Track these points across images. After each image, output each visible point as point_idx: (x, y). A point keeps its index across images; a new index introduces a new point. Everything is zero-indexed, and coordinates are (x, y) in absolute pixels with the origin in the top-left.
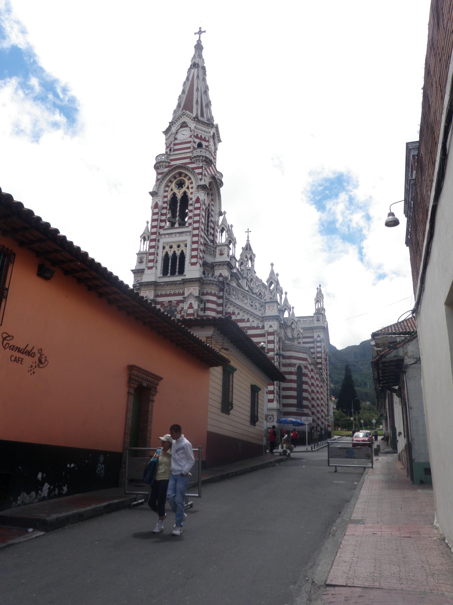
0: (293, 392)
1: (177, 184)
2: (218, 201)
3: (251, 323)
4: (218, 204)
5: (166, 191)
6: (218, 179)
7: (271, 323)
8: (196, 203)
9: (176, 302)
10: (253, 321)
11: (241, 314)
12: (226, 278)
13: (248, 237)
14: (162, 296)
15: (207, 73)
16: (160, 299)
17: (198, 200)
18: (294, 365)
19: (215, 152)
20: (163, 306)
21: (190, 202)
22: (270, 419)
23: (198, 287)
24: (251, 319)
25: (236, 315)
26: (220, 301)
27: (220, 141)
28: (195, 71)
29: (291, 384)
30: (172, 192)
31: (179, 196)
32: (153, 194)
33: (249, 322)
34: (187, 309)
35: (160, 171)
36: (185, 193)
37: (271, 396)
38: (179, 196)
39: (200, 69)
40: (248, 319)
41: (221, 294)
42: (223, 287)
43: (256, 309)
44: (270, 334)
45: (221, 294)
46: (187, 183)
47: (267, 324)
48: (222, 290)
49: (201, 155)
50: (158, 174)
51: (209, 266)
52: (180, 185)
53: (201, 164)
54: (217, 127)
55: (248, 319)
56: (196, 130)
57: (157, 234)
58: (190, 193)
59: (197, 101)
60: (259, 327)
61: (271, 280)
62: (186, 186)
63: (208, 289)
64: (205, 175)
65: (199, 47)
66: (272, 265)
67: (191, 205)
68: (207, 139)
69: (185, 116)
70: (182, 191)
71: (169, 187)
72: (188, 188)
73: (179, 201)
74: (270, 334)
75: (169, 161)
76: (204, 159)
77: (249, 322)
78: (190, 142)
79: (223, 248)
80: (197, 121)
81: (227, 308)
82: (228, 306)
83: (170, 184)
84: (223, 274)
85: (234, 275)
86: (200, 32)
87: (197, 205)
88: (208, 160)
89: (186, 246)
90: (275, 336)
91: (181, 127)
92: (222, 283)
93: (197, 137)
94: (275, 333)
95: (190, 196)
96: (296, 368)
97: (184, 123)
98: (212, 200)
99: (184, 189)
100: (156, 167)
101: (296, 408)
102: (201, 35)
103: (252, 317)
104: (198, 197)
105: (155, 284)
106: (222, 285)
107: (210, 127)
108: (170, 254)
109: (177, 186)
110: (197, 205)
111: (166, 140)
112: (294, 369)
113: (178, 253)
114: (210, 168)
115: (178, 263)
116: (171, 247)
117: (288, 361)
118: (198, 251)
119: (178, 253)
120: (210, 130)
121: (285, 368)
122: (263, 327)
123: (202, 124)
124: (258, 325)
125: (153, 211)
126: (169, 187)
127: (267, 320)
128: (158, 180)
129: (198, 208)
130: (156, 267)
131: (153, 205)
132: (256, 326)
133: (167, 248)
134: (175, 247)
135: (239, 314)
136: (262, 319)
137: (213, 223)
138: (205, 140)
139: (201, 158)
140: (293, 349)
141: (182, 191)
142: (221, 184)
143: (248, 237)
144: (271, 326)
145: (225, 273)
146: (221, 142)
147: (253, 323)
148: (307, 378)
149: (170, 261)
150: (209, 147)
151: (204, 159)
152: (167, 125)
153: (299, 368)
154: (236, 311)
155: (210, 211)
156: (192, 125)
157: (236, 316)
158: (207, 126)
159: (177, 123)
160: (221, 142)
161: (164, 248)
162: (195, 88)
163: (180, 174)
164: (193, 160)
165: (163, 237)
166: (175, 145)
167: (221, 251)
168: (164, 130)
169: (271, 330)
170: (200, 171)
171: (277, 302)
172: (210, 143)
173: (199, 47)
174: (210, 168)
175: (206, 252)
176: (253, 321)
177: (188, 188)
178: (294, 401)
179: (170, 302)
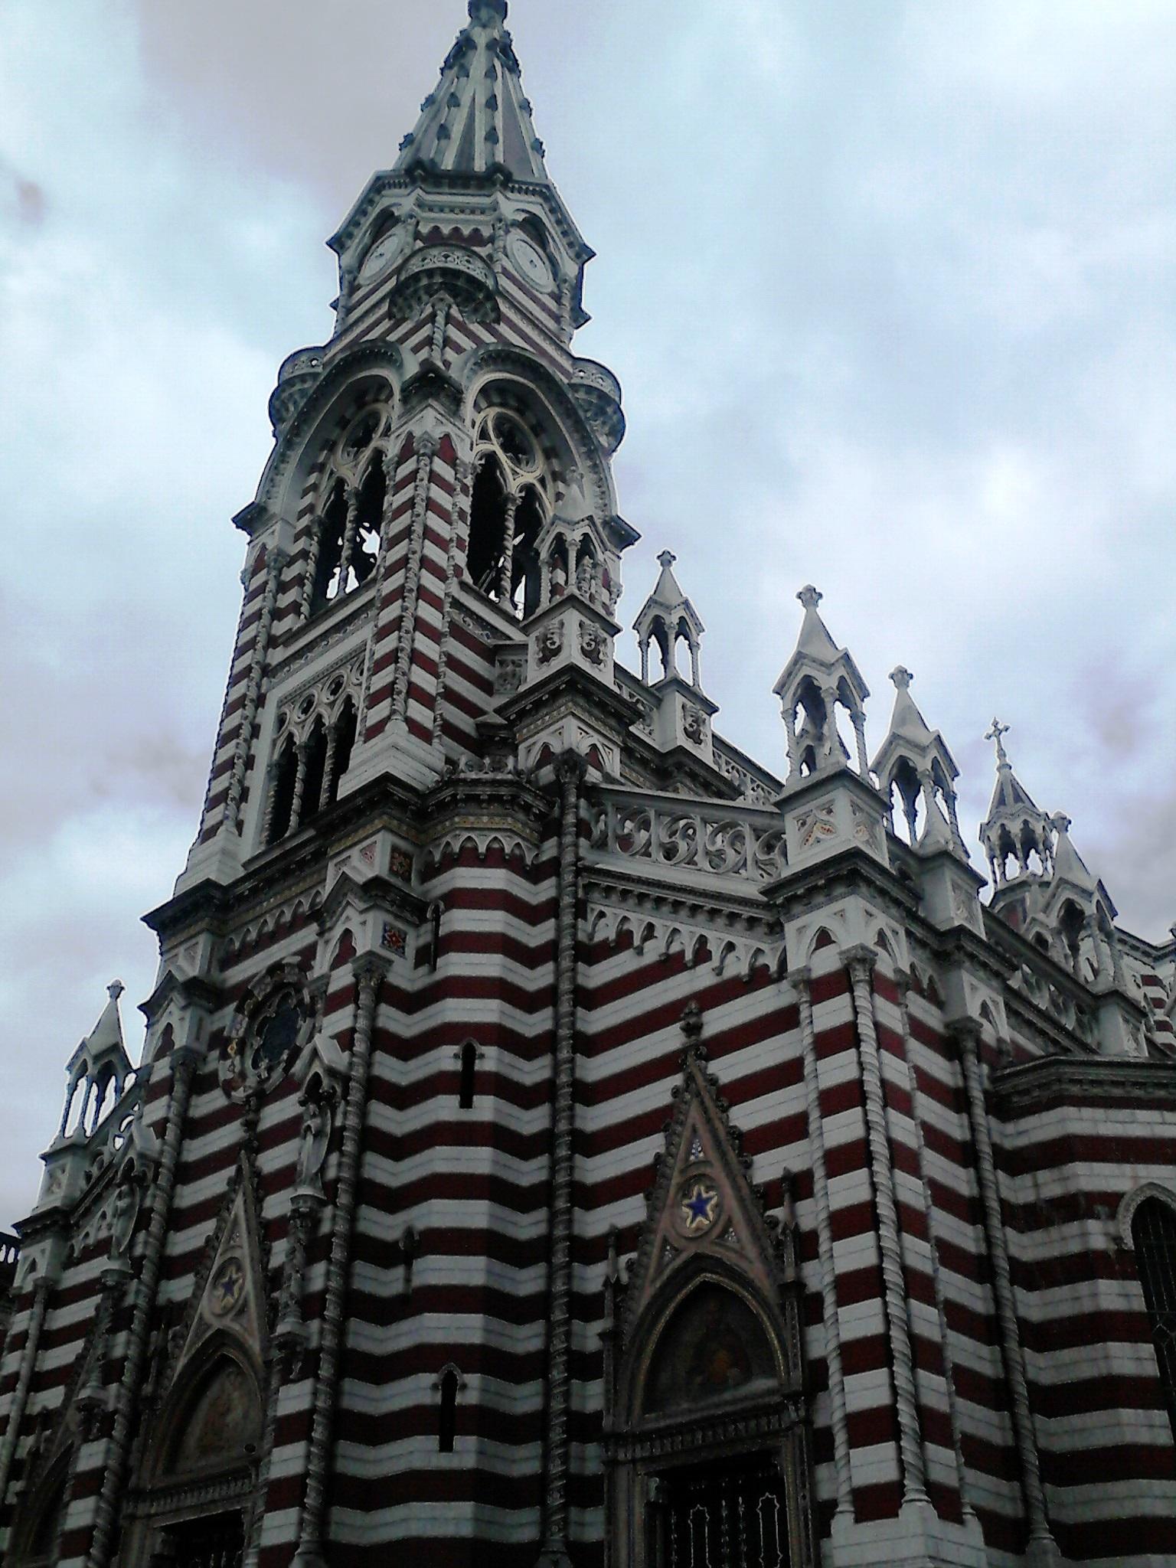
3: (715, 962)
7: (820, 917)
9: (298, 958)
10: (730, 947)
11: (663, 924)
14: (249, 950)
16: (237, 974)
20: (249, 1005)
25: (637, 942)
26: (542, 892)
34: (325, 969)
37: (873, 1464)
40: (702, 940)
41: (549, 849)
44: (822, 989)
45: (549, 849)
48: (549, 827)
60: (767, 967)
61: (806, 671)
64: (447, 341)
66: (810, 597)
68: (486, 232)
70: (367, 453)
71: (321, 468)
74: (822, 989)
81: (591, 917)
84: (557, 748)
85: (679, 766)
88: (460, 283)
90: (862, 991)
92: (556, 790)
94: (860, 974)
96: (1125, 1228)
98: (556, 476)
99: (376, 442)
103: (721, 921)
104: (410, 435)
106: (555, 801)
117: (1050, 1184)
119: (330, 718)
124: (761, 961)
125: (246, 590)
126: (321, 468)
127: (797, 909)
130: (239, 825)
131: (252, 562)
133: (294, 715)
135: (650, 931)
136: (766, 916)
139: (424, 282)
140: (1075, 1090)
141: (367, 453)
144: (824, 938)
145: (572, 732)
147: (731, 957)
157: (640, 951)
161: (281, 721)
165: (281, 675)
169: (826, 963)
171: (844, 775)
174: (503, 328)
176: (730, 947)
179: (276, 968)
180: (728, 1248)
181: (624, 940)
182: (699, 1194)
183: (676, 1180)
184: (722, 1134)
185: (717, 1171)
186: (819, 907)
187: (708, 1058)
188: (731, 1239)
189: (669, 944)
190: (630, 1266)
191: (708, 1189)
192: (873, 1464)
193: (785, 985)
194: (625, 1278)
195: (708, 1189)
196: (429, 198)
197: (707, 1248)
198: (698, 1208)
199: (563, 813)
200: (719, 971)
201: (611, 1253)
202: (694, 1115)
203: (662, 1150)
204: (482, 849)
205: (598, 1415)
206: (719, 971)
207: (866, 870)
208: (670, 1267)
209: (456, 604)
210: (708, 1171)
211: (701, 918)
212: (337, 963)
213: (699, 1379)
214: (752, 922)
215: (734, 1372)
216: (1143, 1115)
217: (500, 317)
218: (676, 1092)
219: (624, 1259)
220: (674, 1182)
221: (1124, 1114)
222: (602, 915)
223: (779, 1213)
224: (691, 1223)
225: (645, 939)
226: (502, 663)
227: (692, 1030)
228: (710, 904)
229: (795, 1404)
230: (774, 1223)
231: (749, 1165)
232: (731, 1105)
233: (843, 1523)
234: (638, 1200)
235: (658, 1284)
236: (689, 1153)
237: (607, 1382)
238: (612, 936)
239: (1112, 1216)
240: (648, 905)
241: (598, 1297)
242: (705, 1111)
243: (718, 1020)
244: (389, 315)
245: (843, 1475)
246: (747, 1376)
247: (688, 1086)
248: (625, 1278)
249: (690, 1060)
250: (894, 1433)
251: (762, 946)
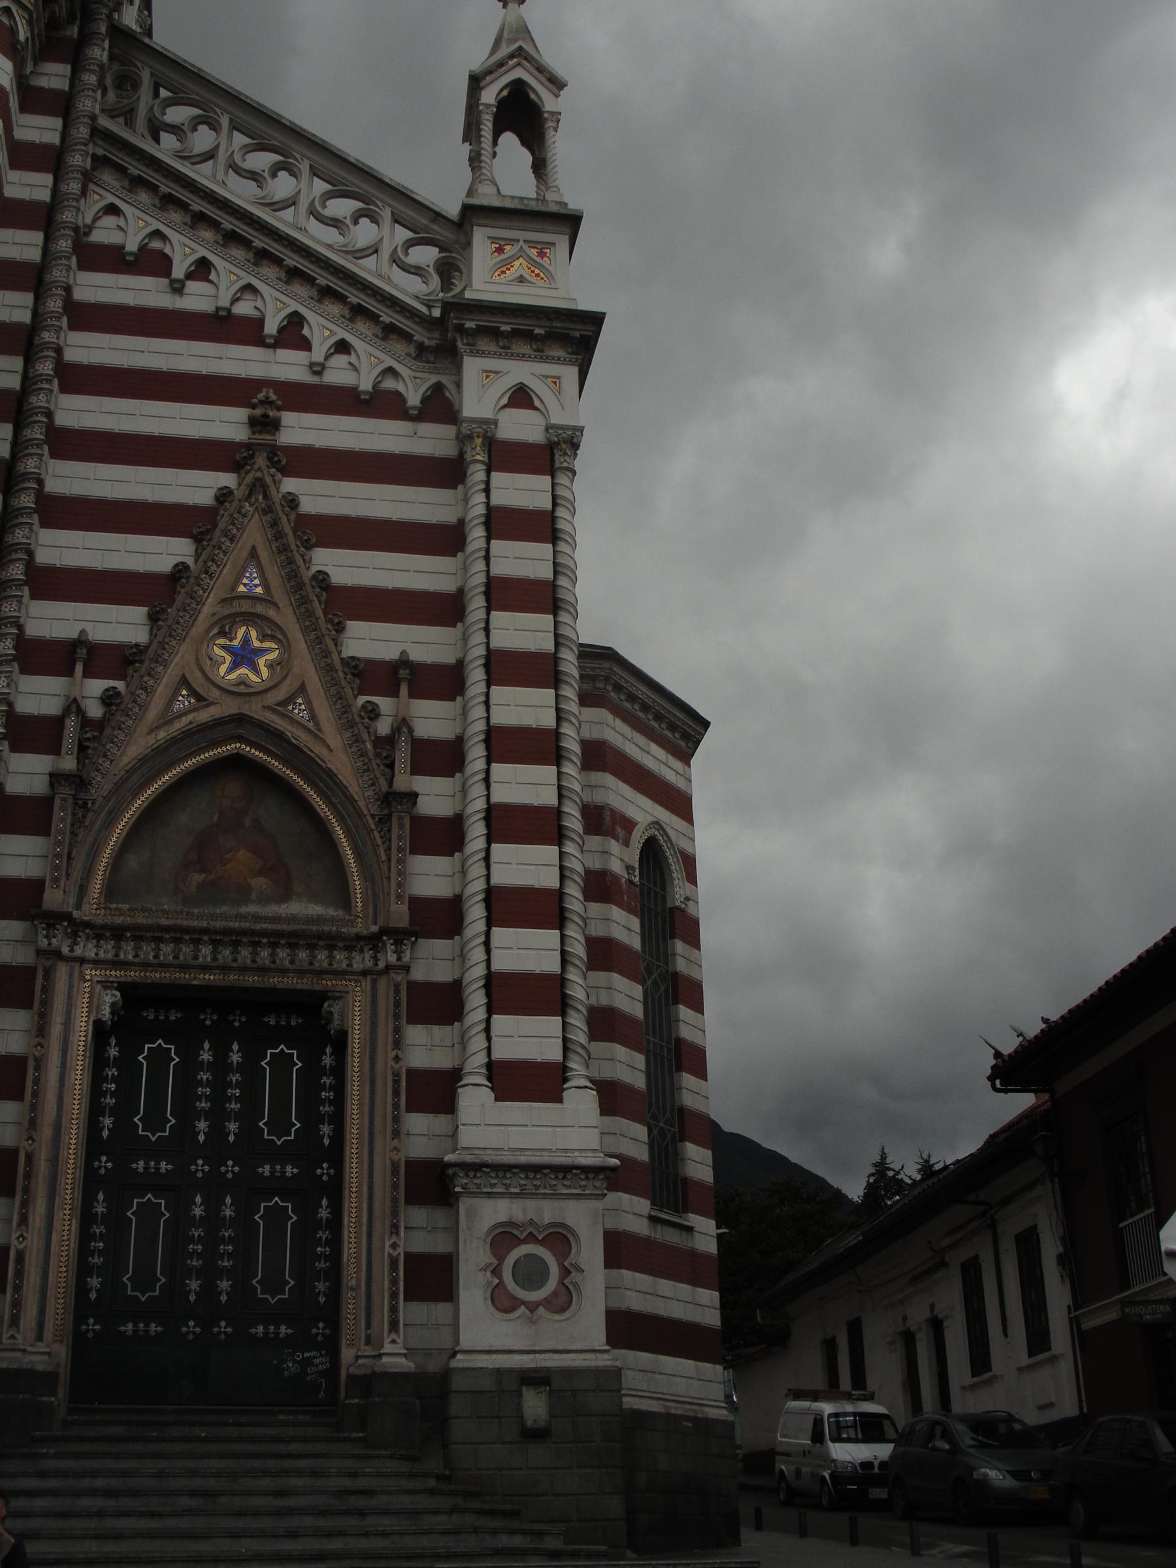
22: (531, 1274)
24: (322, 328)
25: (178, 272)
37: (529, 1037)
40: (295, 321)
55: (295, 321)
60: (398, 398)
101: (643, 1205)
122: (439, 407)
124: (389, 384)
127: (484, 344)
135: (202, 269)
136: (420, 335)
144: (521, 397)
147: (340, 360)
157: (177, 288)
169: (519, 427)
176: (342, 347)
180: (293, 721)
181: (151, 262)
182: (246, 641)
183: (210, 608)
184: (307, 575)
185: (288, 619)
186: (522, 357)
187: (287, 472)
188: (300, 711)
189: (235, 300)
190: (109, 699)
191: (263, 637)
192: (529, 1037)
194: (95, 710)
195: (263, 637)
197: (254, 710)
198: (244, 656)
200: (317, 369)
201: (79, 668)
202: (254, 534)
203: (190, 561)
205: (36, 887)
206: (317, 369)
208: (185, 720)
210: (271, 613)
213: (198, 878)
214: (390, 331)
215: (259, 883)
218: (224, 496)
219: (97, 686)
220: (206, 610)
221: (642, 740)
222: (112, 210)
223: (385, 704)
224: (225, 672)
225: (190, 276)
227: (264, 424)
229: (398, 943)
230: (373, 713)
231: (340, 628)
232: (321, 544)
233: (475, 1099)
234: (142, 611)
235: (162, 734)
236: (237, 581)
237: (59, 843)
238: (132, 246)
241: (57, 723)
242: (279, 536)
243: (301, 429)
245: (478, 1042)
246: (286, 896)
247: (250, 495)
248: (95, 710)
249: (261, 461)
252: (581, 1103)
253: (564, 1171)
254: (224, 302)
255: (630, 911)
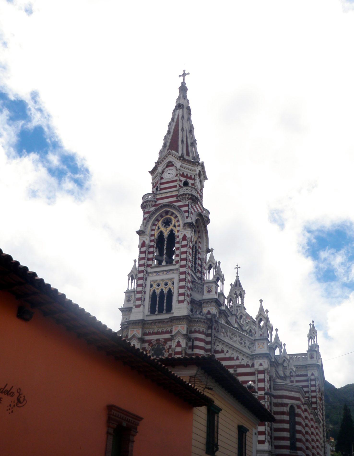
0: (285, 433)
1: (164, 223)
2: (205, 238)
3: (240, 361)
4: (205, 241)
5: (153, 230)
6: (205, 216)
7: (261, 361)
8: (183, 240)
9: (164, 340)
12: (214, 316)
13: (237, 273)
14: (149, 334)
15: (191, 113)
16: (148, 338)
17: (184, 238)
18: (286, 405)
19: (201, 190)
20: (151, 345)
21: (177, 240)
23: (185, 325)
24: (240, 357)
25: (225, 352)
26: (209, 339)
27: (206, 178)
28: (180, 112)
29: (283, 424)
30: (159, 230)
31: (166, 234)
32: (140, 233)
33: (238, 359)
34: (174, 347)
35: (147, 210)
36: (172, 231)
37: (262, 438)
38: (166, 234)
39: (185, 109)
40: (238, 357)
41: (209, 331)
42: (211, 325)
43: (245, 346)
44: (260, 372)
45: (209, 331)
46: (174, 221)
47: (257, 363)
48: (210, 328)
49: (187, 193)
50: (145, 213)
51: (197, 304)
52: (167, 223)
53: (187, 202)
54: (202, 165)
55: (238, 357)
56: (182, 169)
57: (145, 273)
58: (177, 231)
59: (182, 141)
60: (249, 365)
62: (173, 224)
63: (196, 327)
64: (191, 212)
65: (183, 89)
66: (261, 301)
67: (178, 242)
68: (193, 177)
69: (170, 156)
70: (169, 229)
71: (156, 225)
72: (175, 226)
73: (166, 239)
74: (260, 372)
75: (155, 200)
76: (190, 196)
77: (238, 359)
78: (176, 181)
79: (211, 285)
80: (182, 160)
81: (216, 345)
82: (217, 343)
83: (156, 223)
84: (211, 312)
86: (184, 75)
87: (184, 243)
88: (194, 198)
89: (173, 284)
90: (266, 374)
91: (167, 166)
92: (211, 320)
93: (183, 175)
94: (266, 372)
95: (177, 234)
97: (170, 162)
98: (199, 237)
99: (171, 227)
100: (143, 206)
101: (289, 451)
102: (185, 77)
103: (241, 355)
104: (185, 235)
105: (142, 322)
107: (196, 165)
108: (158, 292)
109: (164, 225)
110: (184, 243)
111: (153, 179)
112: (286, 409)
113: (166, 291)
114: (197, 205)
115: (165, 301)
116: (158, 285)
117: (280, 401)
118: (185, 288)
119: (166, 291)
120: (196, 168)
121: (277, 408)
122: (253, 366)
123: (187, 163)
124: (248, 363)
125: (140, 250)
126: (156, 225)
128: (144, 219)
129: (185, 246)
130: (144, 306)
131: (141, 244)
132: (245, 364)
133: (155, 286)
134: (162, 284)
135: (227, 352)
137: (201, 261)
138: (191, 178)
139: (187, 196)
140: (285, 388)
141: (169, 229)
142: (208, 221)
143: (237, 273)
144: (261, 365)
146: (207, 179)
147: (243, 361)
148: (300, 418)
149: (158, 299)
150: (195, 185)
151: (190, 196)
152: (153, 165)
153: (292, 407)
154: (225, 349)
155: (198, 248)
156: (178, 164)
157: (225, 355)
158: (193, 164)
159: (162, 163)
160: (207, 179)
161: (151, 286)
162: (180, 128)
163: (167, 212)
164: (179, 198)
165: (150, 275)
166: (161, 184)
167: (209, 288)
168: (151, 170)
169: (261, 368)
170: (186, 208)
172: (196, 181)
173: (183, 89)
174: (197, 205)
175: (194, 289)
176: (243, 359)
177: (175, 226)
178: (287, 443)
179: (158, 340)
181: (222, 352)
193: (252, 368)
196: (183, 165)
199: (212, 325)
200: (241, 363)
204: (201, 331)
206: (241, 363)
207: (269, 356)
209: (192, 275)
211: (238, 353)
212: (177, 346)
216: (293, 393)
217: (197, 203)
222: (218, 345)
226: (194, 285)
228: (240, 351)
239: (287, 407)
240: (228, 347)
244: (176, 196)
250: (265, 434)
251: (249, 361)
252: (267, 444)
253: (265, 451)
254: (230, 356)
255: (287, 415)
